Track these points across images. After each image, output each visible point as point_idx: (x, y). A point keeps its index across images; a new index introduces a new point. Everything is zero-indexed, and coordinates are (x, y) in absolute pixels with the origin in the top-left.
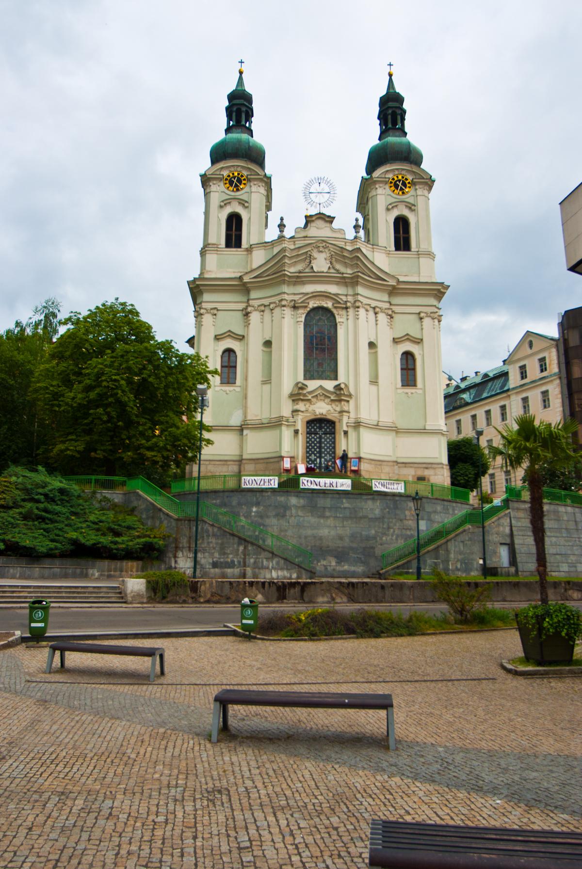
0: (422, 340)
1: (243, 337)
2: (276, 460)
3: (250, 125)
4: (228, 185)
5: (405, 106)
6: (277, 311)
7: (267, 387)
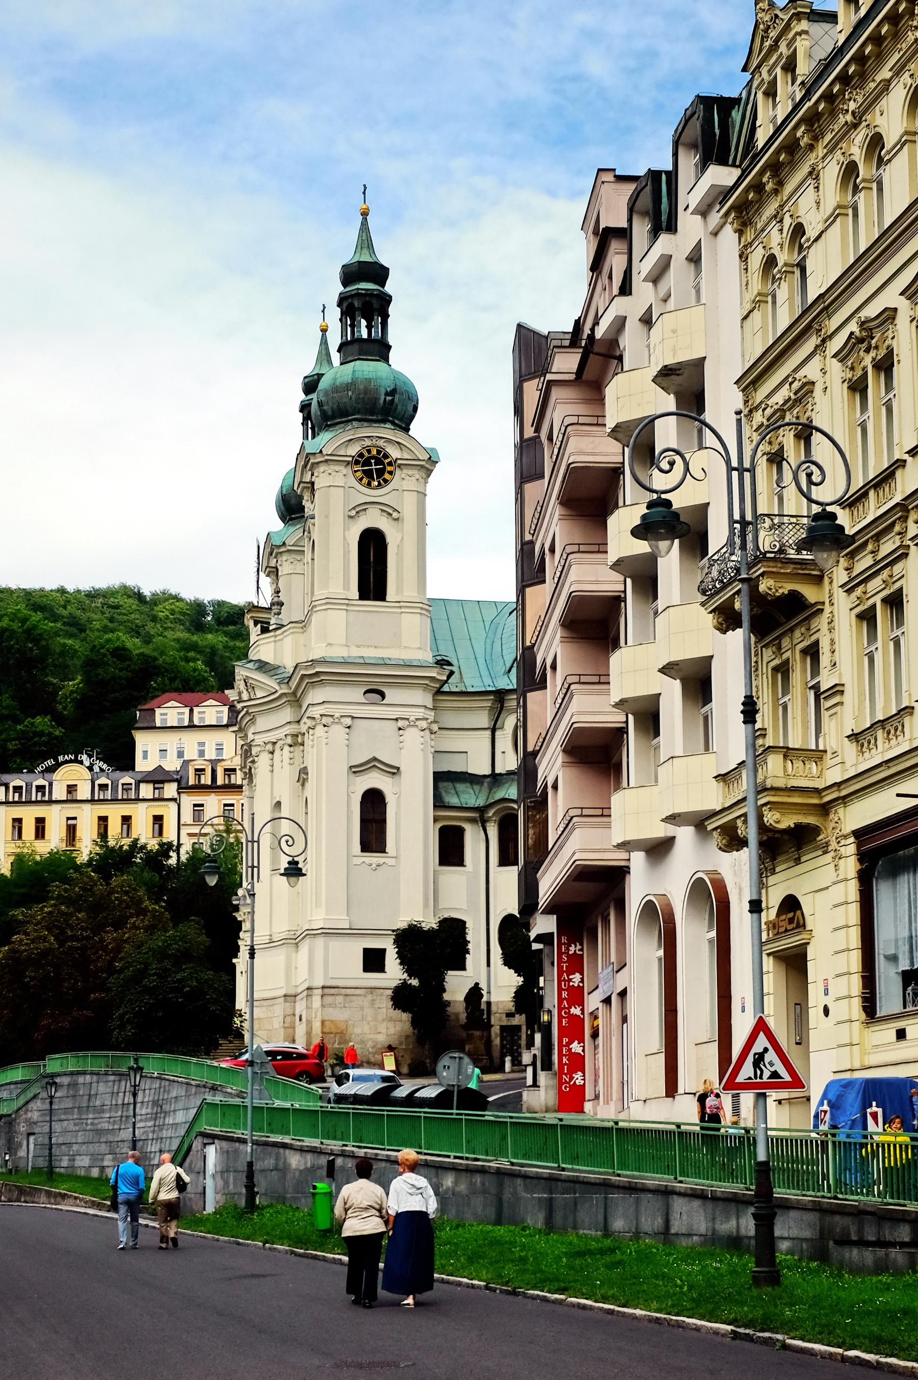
0: (398, 769)
5: (390, 287)
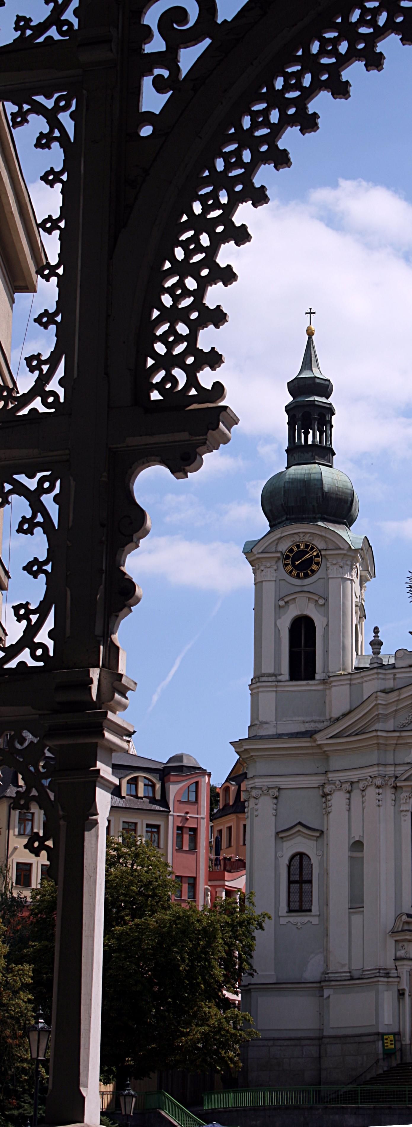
1: (322, 832)
2: (371, 1038)
3: (329, 438)
4: (290, 567)
6: (372, 792)
7: (356, 919)
